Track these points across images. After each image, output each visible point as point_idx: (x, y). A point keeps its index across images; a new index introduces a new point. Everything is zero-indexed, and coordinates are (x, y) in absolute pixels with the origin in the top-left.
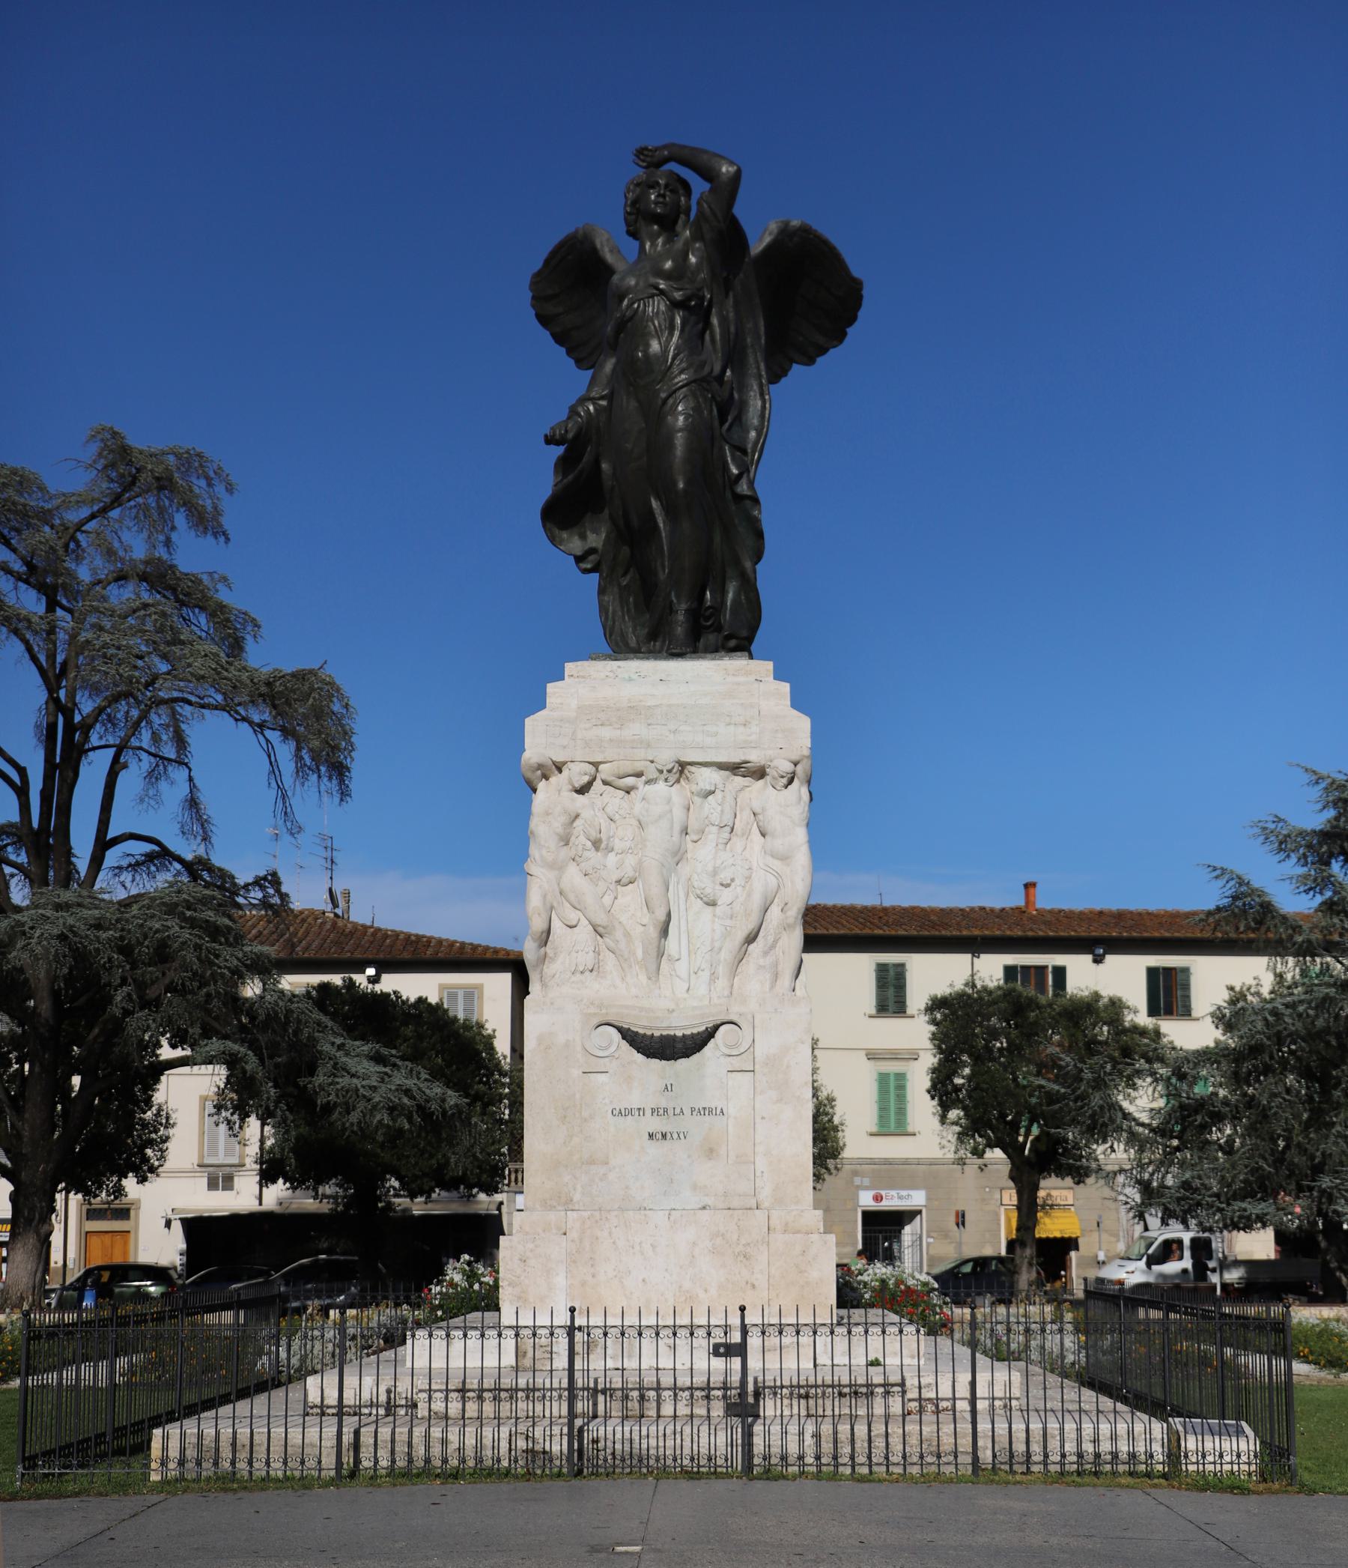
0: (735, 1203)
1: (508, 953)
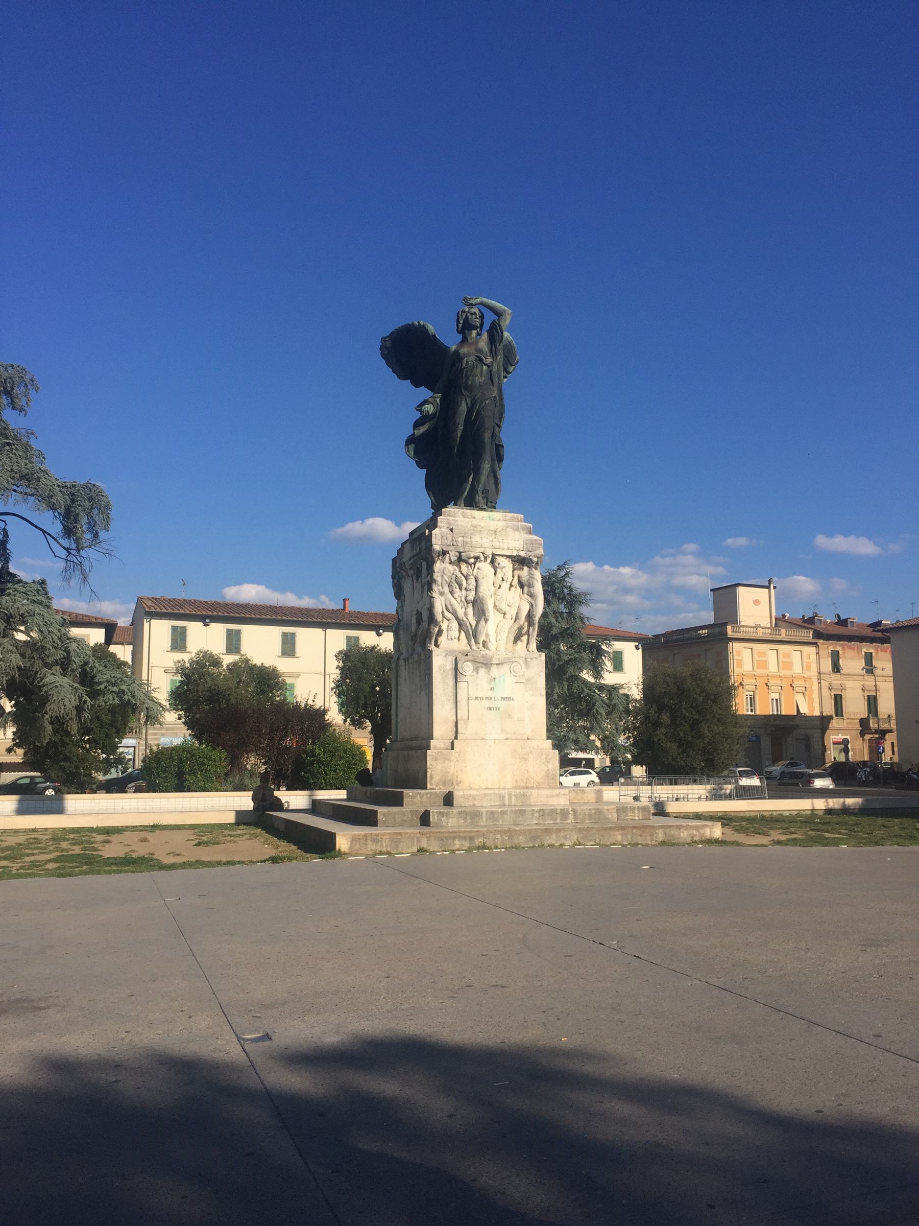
1: (102, 619)
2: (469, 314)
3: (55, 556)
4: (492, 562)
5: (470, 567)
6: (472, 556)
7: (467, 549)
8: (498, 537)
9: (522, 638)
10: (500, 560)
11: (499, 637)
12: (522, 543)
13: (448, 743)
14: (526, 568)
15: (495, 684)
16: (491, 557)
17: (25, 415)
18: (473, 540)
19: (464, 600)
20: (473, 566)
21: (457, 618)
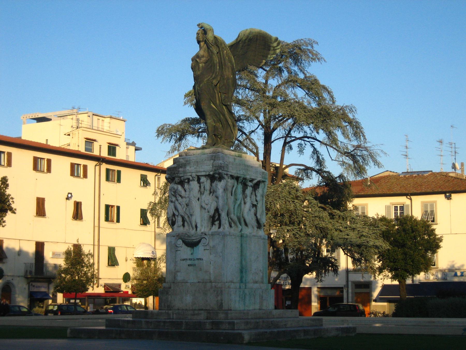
9: (215, 223)
15: (194, 251)
16: (196, 177)
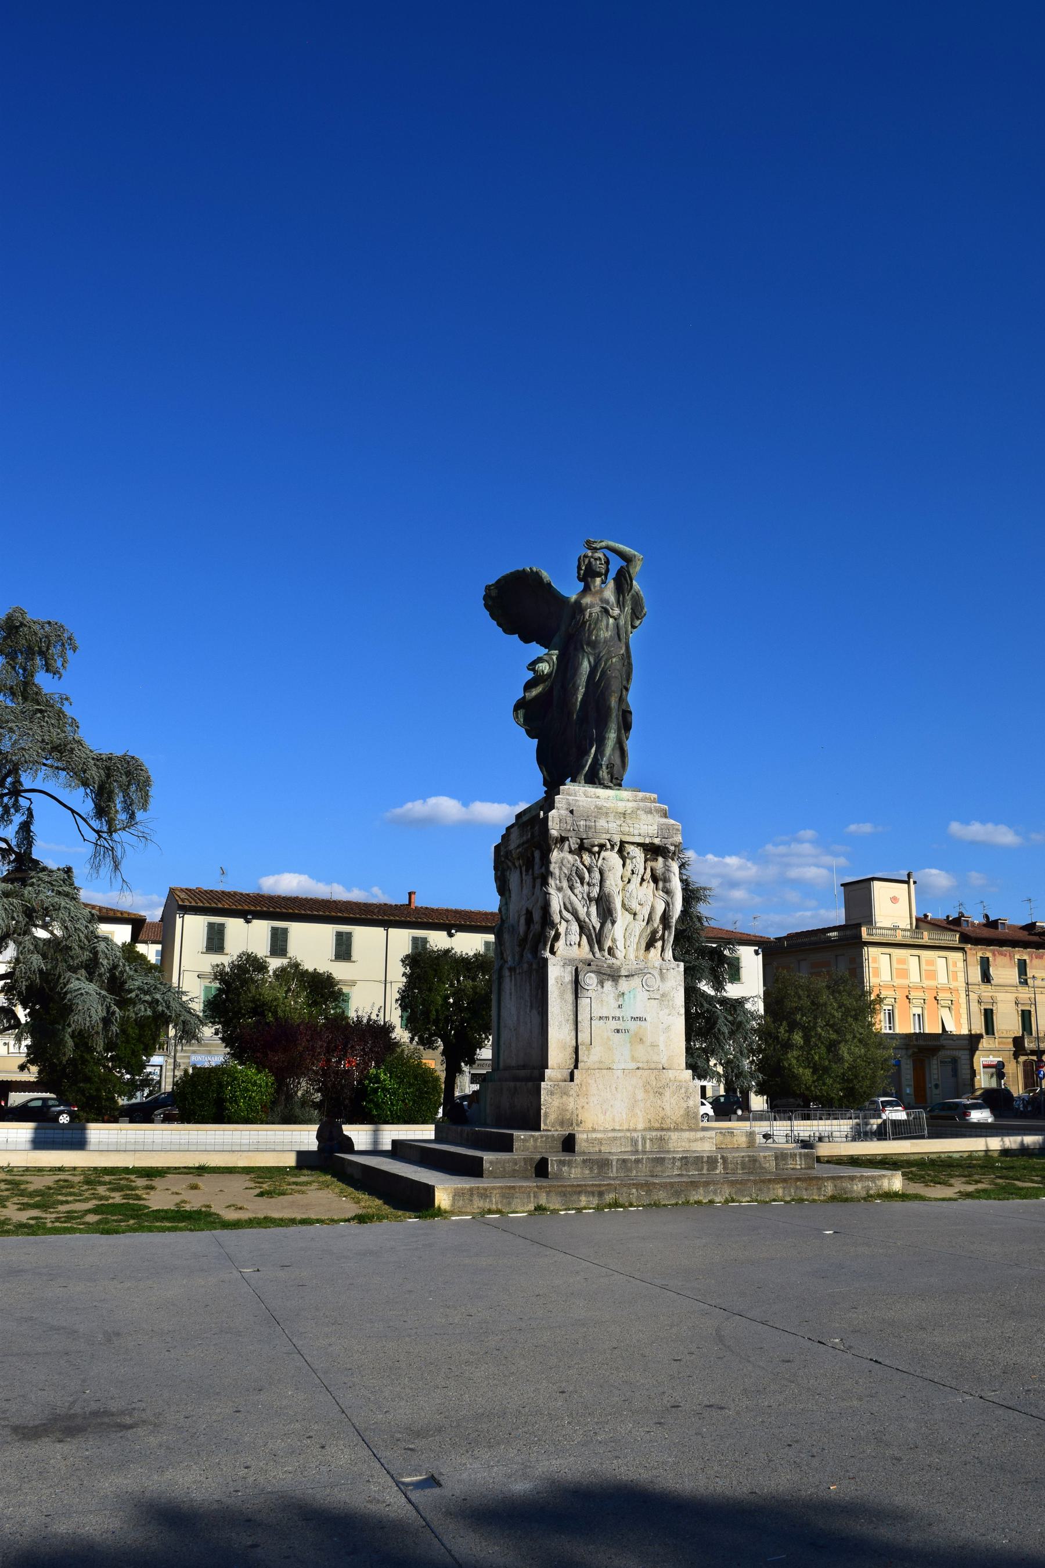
0: (653, 1066)
1: (129, 914)
2: (592, 560)
3: (84, 840)
4: (620, 852)
5: (593, 857)
6: (596, 843)
7: (590, 835)
8: (629, 821)
9: (656, 944)
10: (630, 848)
11: (628, 943)
12: (656, 828)
13: (566, 1073)
14: (660, 859)
17: (60, 678)
18: (597, 824)
19: (585, 897)
20: (597, 855)
21: (578, 919)
